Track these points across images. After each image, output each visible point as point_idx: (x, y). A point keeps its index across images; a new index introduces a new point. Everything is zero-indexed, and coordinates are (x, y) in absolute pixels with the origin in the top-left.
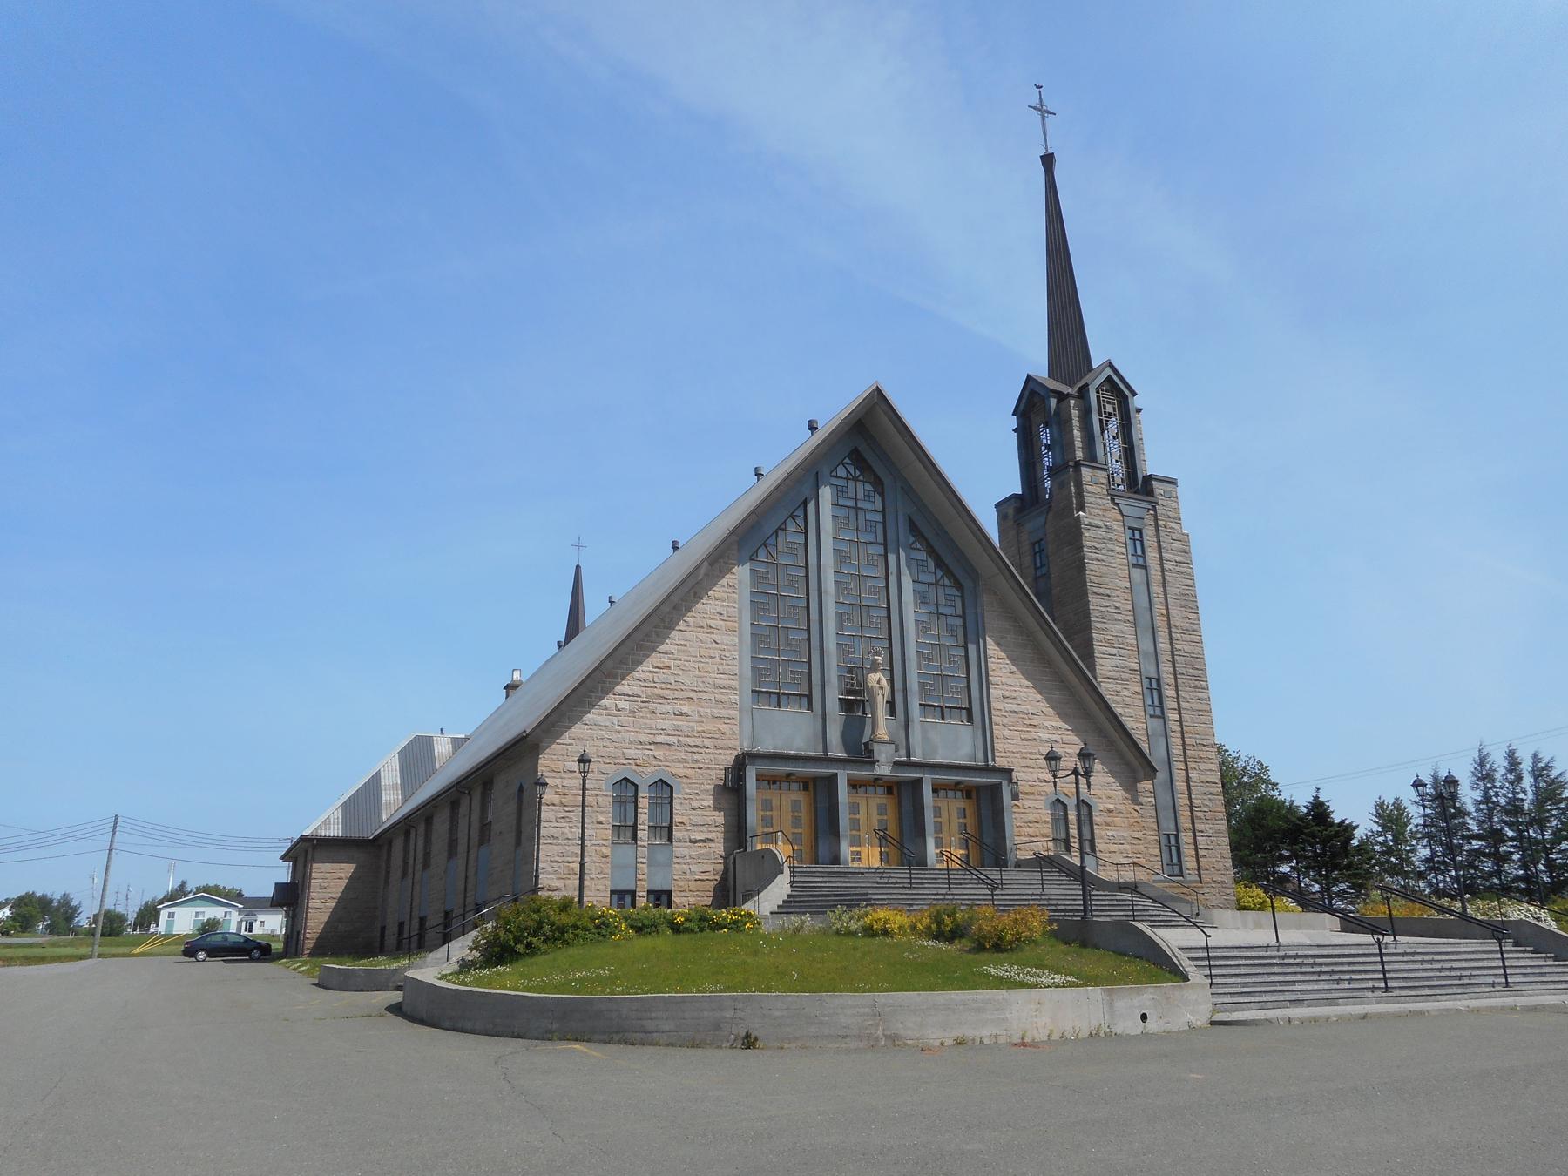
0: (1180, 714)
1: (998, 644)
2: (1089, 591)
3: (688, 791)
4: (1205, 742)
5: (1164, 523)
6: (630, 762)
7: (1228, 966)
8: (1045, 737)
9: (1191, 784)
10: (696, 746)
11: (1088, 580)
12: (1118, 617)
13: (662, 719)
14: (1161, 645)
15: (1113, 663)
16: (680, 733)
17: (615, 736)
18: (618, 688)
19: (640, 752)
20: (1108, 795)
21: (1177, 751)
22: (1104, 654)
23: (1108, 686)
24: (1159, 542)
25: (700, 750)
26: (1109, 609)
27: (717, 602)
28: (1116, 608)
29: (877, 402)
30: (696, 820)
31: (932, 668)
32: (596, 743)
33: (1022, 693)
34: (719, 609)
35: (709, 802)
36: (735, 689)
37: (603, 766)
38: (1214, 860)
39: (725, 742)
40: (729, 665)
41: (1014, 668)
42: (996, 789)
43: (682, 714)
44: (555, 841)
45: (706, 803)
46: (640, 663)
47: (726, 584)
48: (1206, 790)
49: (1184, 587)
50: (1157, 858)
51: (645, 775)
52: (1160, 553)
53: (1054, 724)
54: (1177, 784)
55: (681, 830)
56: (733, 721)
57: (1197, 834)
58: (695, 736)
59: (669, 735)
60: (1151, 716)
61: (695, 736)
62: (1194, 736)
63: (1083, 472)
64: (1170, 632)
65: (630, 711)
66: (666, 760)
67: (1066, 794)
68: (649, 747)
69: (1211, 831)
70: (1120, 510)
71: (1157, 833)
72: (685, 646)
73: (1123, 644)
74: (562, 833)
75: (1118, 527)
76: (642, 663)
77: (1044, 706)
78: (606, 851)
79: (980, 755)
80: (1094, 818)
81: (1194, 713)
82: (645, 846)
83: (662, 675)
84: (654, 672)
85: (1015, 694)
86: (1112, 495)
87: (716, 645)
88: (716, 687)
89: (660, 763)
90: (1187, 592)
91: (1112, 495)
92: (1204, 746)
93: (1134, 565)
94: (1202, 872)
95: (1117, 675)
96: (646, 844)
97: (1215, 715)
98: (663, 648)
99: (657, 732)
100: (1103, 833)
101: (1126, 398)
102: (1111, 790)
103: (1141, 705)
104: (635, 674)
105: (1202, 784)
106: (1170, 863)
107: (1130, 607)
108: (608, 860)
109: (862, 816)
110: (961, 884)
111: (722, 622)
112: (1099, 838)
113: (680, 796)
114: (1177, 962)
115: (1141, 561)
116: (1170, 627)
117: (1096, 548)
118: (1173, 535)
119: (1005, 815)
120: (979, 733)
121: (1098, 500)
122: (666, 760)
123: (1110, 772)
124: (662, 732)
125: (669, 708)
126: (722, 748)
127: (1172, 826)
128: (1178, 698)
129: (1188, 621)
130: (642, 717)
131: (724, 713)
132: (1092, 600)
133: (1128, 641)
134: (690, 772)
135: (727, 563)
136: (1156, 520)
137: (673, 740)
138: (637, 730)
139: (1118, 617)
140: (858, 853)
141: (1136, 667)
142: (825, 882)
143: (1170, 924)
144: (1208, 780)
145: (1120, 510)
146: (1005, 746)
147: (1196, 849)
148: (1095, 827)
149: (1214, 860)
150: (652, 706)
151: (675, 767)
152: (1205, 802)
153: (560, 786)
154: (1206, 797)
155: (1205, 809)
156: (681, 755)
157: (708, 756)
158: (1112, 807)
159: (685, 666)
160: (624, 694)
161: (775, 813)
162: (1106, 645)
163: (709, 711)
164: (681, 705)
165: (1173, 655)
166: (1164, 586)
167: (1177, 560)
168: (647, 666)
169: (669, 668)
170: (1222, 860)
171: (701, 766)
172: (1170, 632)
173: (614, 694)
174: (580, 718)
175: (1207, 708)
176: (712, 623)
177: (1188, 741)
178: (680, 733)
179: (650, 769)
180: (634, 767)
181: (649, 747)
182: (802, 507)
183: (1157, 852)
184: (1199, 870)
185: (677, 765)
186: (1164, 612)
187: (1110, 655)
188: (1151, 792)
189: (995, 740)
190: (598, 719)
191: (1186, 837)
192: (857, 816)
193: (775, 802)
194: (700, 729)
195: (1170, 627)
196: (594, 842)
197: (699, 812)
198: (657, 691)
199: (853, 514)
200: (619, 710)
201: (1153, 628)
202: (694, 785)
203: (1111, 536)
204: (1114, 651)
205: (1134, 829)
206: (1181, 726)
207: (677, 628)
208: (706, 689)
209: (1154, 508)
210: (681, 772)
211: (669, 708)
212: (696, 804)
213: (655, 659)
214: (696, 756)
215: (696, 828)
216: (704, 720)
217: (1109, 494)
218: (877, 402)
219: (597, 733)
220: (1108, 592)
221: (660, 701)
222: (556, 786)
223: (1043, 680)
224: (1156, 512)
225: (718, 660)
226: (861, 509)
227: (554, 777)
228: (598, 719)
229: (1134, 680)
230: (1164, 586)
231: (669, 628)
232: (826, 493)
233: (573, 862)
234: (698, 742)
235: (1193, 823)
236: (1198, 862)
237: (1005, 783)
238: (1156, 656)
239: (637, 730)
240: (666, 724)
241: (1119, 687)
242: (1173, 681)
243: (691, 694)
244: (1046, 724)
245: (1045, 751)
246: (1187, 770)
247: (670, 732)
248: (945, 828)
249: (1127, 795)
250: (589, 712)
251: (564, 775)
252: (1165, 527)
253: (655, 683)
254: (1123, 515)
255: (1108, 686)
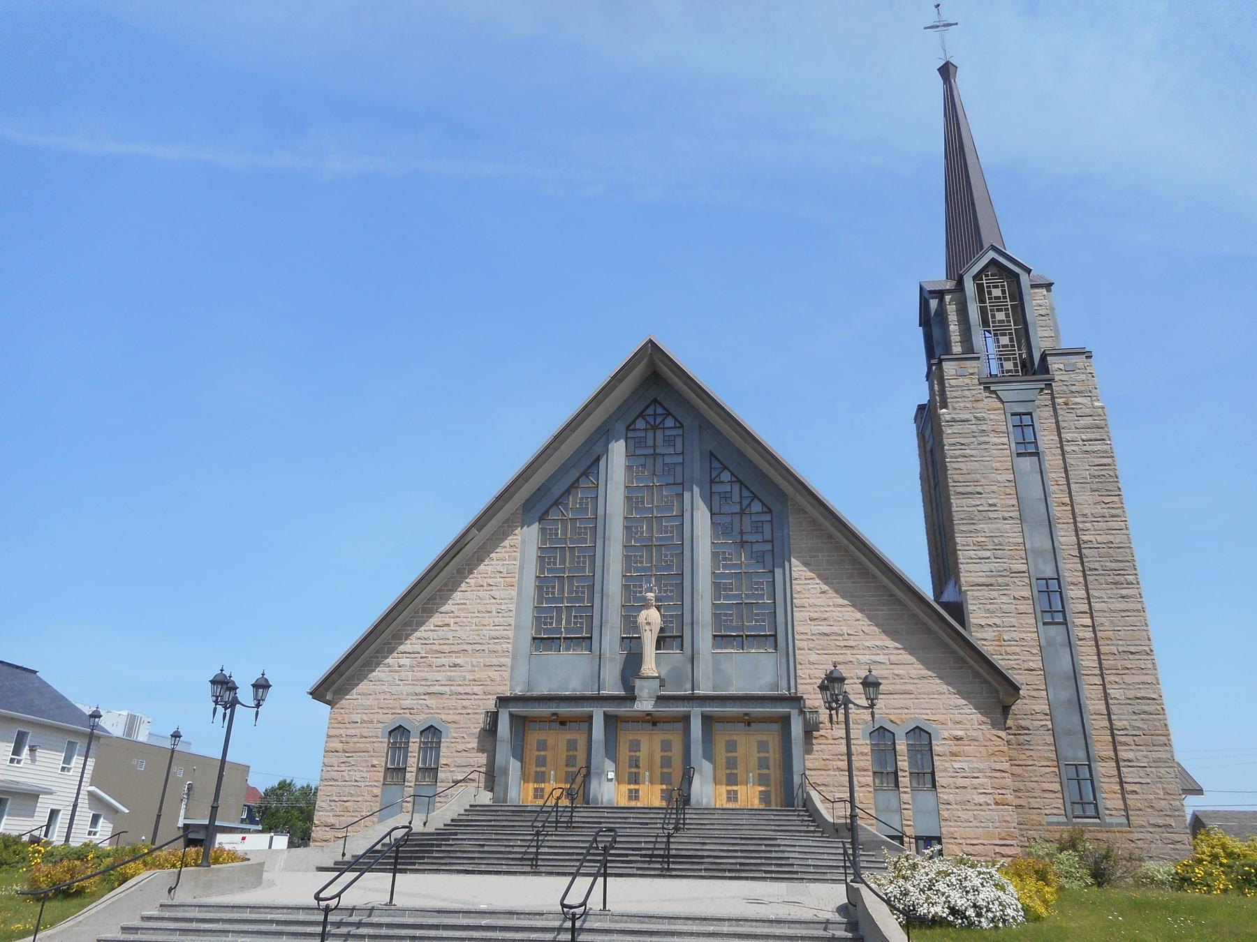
0: (1092, 618)
1: (806, 564)
2: (952, 493)
3: (455, 735)
4: (1133, 649)
5: (1064, 400)
6: (405, 711)
7: (210, 931)
8: (863, 658)
9: (1110, 701)
10: (466, 693)
11: (950, 480)
12: (992, 515)
13: (438, 671)
14: (1062, 539)
15: (985, 567)
16: (451, 683)
17: (394, 689)
18: (402, 648)
19: (414, 702)
20: (957, 720)
21: (1088, 661)
22: (972, 559)
23: (976, 594)
24: (1057, 422)
25: (469, 697)
26: (981, 508)
27: (498, 562)
28: (991, 505)
29: (652, 356)
30: (459, 761)
31: (735, 597)
32: (379, 696)
33: (836, 614)
34: (499, 568)
35: (474, 744)
36: (509, 638)
37: (381, 716)
38: (1152, 797)
39: (494, 688)
40: (505, 617)
41: (826, 588)
42: (785, 721)
43: (455, 666)
44: (335, 783)
45: (470, 746)
46: (422, 624)
47: (508, 546)
48: (1136, 708)
49: (1096, 468)
50: (1057, 795)
51: (417, 722)
52: (1059, 434)
53: (878, 643)
54: (1088, 702)
55: (445, 771)
56: (504, 668)
57: (1122, 764)
58: (466, 685)
59: (442, 685)
60: (1045, 624)
61: (466, 685)
62: (1115, 642)
63: (944, 367)
64: (1075, 522)
65: (410, 666)
66: (437, 708)
67: (892, 721)
68: (423, 697)
69: (1146, 760)
70: (998, 398)
71: (1055, 763)
72: (465, 604)
73: (1000, 544)
74: (342, 776)
75: (997, 416)
76: (424, 624)
77: (865, 624)
78: (377, 791)
79: (784, 684)
80: (934, 747)
81: (1115, 614)
82: (411, 787)
83: (441, 633)
84: (434, 631)
85: (825, 615)
86: (984, 383)
87: (494, 601)
88: (490, 639)
89: (432, 711)
90: (1103, 473)
91: (984, 383)
92: (1132, 653)
93: (1019, 455)
94: (1130, 813)
95: (992, 580)
96: (412, 784)
97: (1150, 615)
98: (443, 609)
99: (431, 683)
100: (947, 765)
101: (1017, 276)
102: (961, 714)
103: (1031, 611)
104: (417, 634)
105: (1129, 702)
106: (1078, 800)
107: (1014, 502)
108: (378, 799)
109: (643, 754)
110: (647, 824)
111: (502, 580)
112: (941, 771)
113: (447, 740)
114: (69, 919)
115: (1031, 449)
116: (1074, 518)
117: (963, 444)
118: (1078, 411)
119: (793, 746)
120: (784, 660)
121: (967, 393)
122: (437, 708)
123: (960, 693)
124: (436, 683)
125: (444, 661)
126: (490, 694)
127: (1081, 754)
128: (1088, 598)
129: (1104, 506)
130: (420, 671)
131: (495, 661)
132: (955, 502)
133: (1011, 540)
134: (457, 718)
135: (510, 527)
136: (1053, 399)
137: (446, 689)
138: (414, 682)
139: (992, 515)
140: (637, 791)
141: (1024, 568)
142: (491, 821)
143: (795, 876)
144: (1139, 695)
145: (998, 398)
146: (811, 672)
147: (1121, 783)
148: (935, 758)
149: (1152, 797)
150: (430, 660)
151: (441, 717)
152: (1134, 723)
153: (344, 736)
154: (1135, 717)
155: (1134, 733)
156: (451, 703)
157: (477, 702)
158: (961, 733)
159: (463, 622)
160: (405, 653)
161: (549, 753)
162: (975, 548)
163: (482, 660)
164: (456, 657)
165: (1080, 549)
166: (1066, 471)
167: (1084, 437)
168: (430, 625)
169: (448, 625)
170: (1167, 797)
171: (469, 711)
172: (1075, 522)
173: (397, 653)
174: (365, 677)
175: (1139, 606)
176: (491, 581)
177: (1103, 649)
178: (451, 683)
179: (422, 717)
180: (408, 716)
181: (423, 697)
182: (713, 459)
183: (1057, 787)
184: (1126, 810)
185: (447, 712)
186: (1067, 500)
187: (980, 559)
188: (1046, 714)
189: (798, 666)
190: (381, 675)
191: (1104, 769)
192: (638, 754)
193: (550, 742)
194: (472, 678)
195: (1074, 518)
196: (367, 784)
197: (464, 754)
198: (434, 647)
199: (650, 461)
200: (400, 667)
201: (1049, 522)
202: (461, 730)
203: (984, 427)
204: (988, 554)
205: (996, 759)
206: (1094, 631)
207: (459, 589)
208: (481, 641)
209: (1049, 386)
210: (450, 718)
211: (444, 661)
212: (460, 747)
213: (436, 619)
214: (466, 703)
215: (460, 769)
216: (476, 669)
217: (980, 384)
218: (652, 356)
219: (378, 688)
220: (979, 489)
221: (437, 656)
222: (341, 735)
223: (865, 596)
224: (1052, 390)
225: (494, 614)
226: (660, 454)
227: (340, 728)
228: (381, 675)
229: (1019, 583)
230: (1066, 471)
231: (451, 590)
232: (618, 449)
233: (348, 801)
234: (468, 690)
235: (1115, 751)
236: (1124, 799)
237: (794, 713)
238: (1054, 552)
239: (414, 682)
240: (439, 676)
241: (995, 594)
242: (1081, 580)
243: (465, 647)
244: (867, 644)
245: (864, 673)
246: (1104, 685)
247: (443, 683)
248: (740, 764)
249: (985, 719)
250: (374, 671)
251: (348, 725)
252: (1066, 404)
253: (434, 640)
254: (1003, 402)
255: (976, 594)
